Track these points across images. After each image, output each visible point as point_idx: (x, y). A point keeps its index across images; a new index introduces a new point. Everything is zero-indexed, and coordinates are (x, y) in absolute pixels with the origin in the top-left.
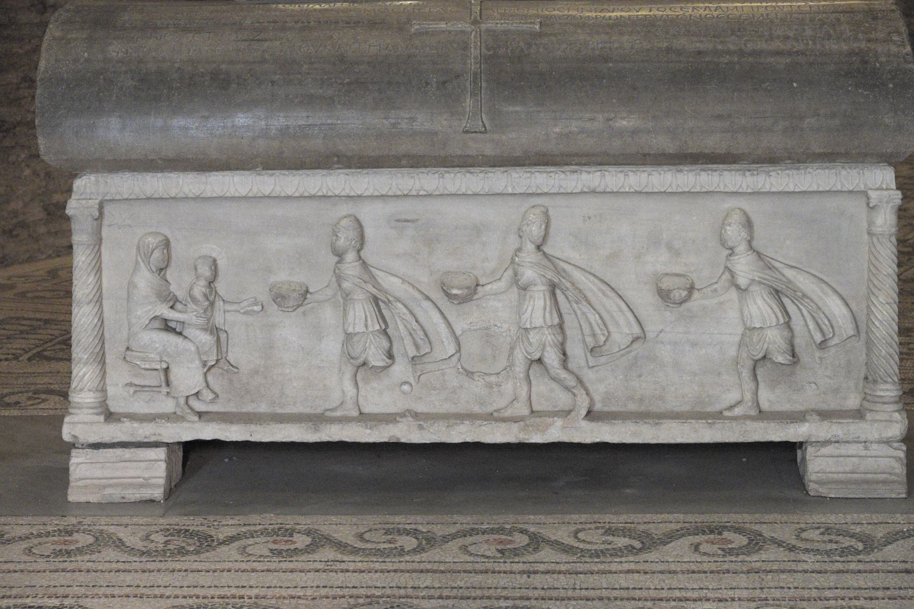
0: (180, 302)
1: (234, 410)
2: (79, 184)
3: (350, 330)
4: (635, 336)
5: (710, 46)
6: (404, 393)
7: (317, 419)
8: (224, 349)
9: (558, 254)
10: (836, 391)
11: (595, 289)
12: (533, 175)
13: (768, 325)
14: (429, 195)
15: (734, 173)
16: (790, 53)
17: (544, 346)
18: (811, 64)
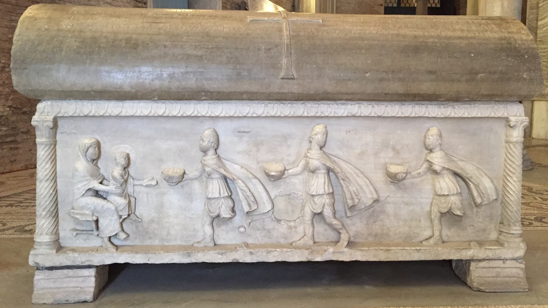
0: (107, 180)
1: (139, 244)
2: (40, 106)
3: (210, 196)
4: (375, 199)
5: (421, 34)
6: (241, 232)
7: (188, 249)
8: (133, 208)
9: (331, 152)
10: (484, 230)
11: (352, 172)
12: (319, 106)
13: (452, 193)
14: (258, 117)
15: (434, 106)
16: (466, 38)
17: (324, 205)
18: (480, 44)
